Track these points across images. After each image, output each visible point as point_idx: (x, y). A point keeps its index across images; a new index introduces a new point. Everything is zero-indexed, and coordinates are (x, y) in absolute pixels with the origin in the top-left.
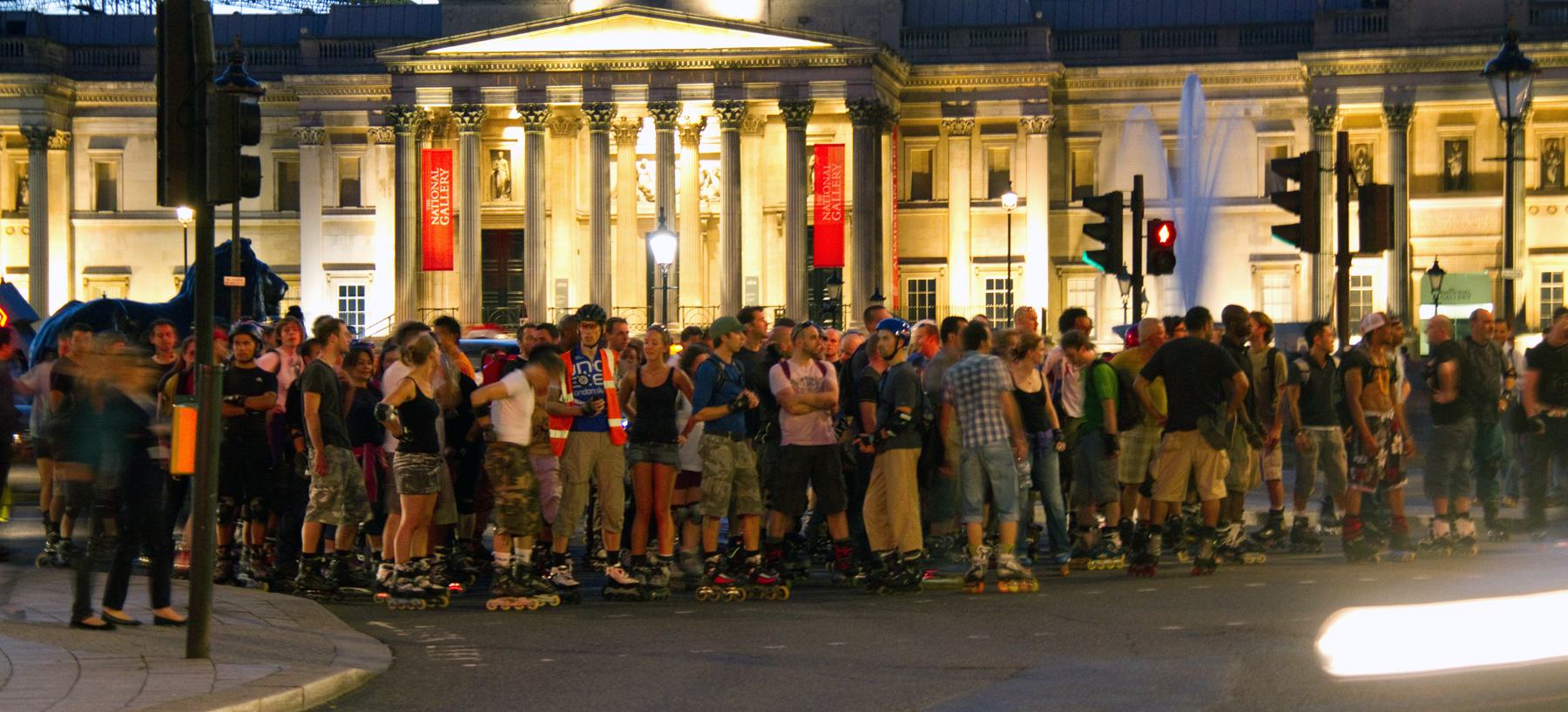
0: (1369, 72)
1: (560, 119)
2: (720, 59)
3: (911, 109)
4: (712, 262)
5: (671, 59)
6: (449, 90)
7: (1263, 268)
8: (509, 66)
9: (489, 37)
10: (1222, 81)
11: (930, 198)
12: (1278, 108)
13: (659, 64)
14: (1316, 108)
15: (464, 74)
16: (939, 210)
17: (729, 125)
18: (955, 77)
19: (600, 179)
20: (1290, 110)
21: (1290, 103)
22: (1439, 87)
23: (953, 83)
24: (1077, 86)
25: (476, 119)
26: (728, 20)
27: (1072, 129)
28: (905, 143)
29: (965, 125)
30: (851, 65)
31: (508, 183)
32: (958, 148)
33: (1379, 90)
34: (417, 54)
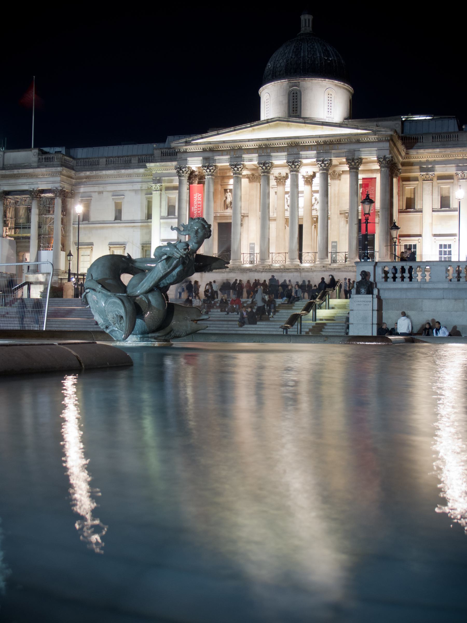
2: (319, 140)
3: (406, 169)
5: (297, 140)
6: (201, 158)
8: (226, 147)
9: (218, 134)
11: (414, 209)
13: (292, 143)
15: (208, 151)
17: (323, 169)
23: (425, 157)
25: (212, 171)
26: (323, 122)
28: (403, 185)
29: (430, 176)
32: (427, 186)
34: (187, 143)
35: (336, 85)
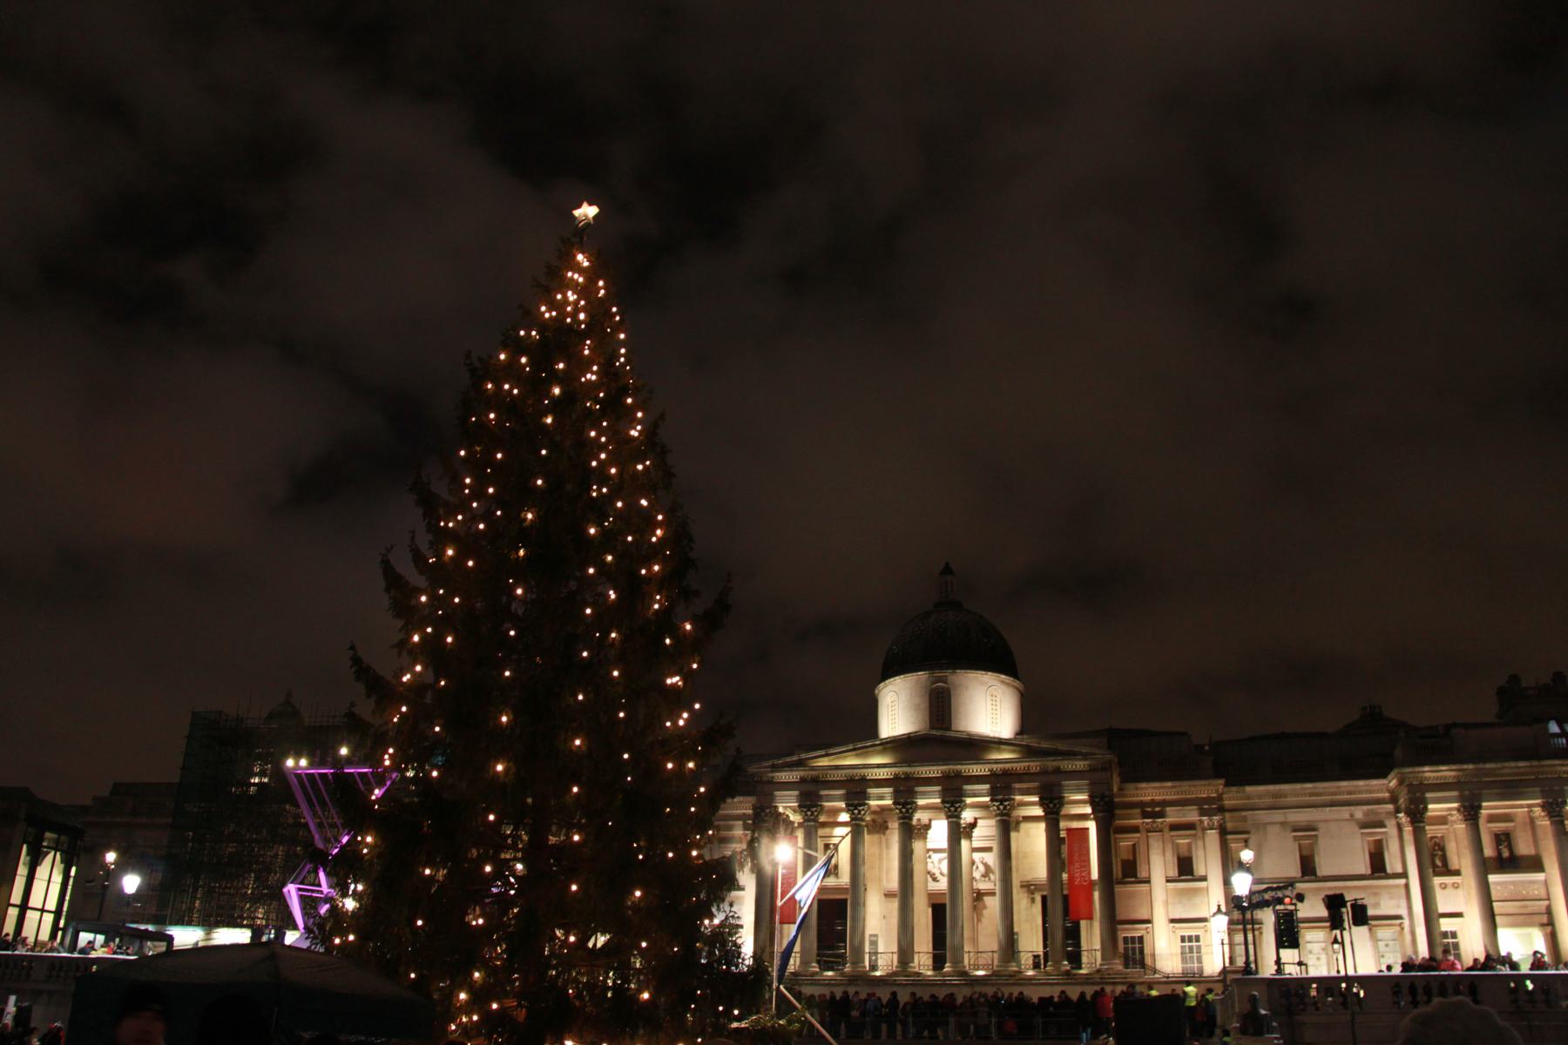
0: (1446, 781)
1: (874, 821)
4: (980, 924)
6: (796, 793)
7: (1376, 926)
9: (827, 755)
10: (1332, 794)
12: (1372, 811)
14: (1412, 807)
16: (1143, 885)
17: (1002, 814)
18: (1150, 792)
19: (906, 856)
20: (1381, 813)
21: (1381, 808)
22: (1497, 791)
24: (1230, 799)
27: (1229, 830)
30: (1092, 770)
31: (836, 867)
33: (1455, 793)
35: (1003, 682)
